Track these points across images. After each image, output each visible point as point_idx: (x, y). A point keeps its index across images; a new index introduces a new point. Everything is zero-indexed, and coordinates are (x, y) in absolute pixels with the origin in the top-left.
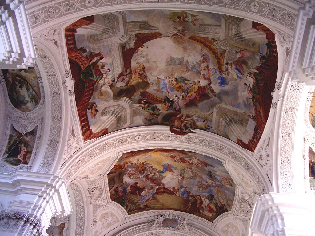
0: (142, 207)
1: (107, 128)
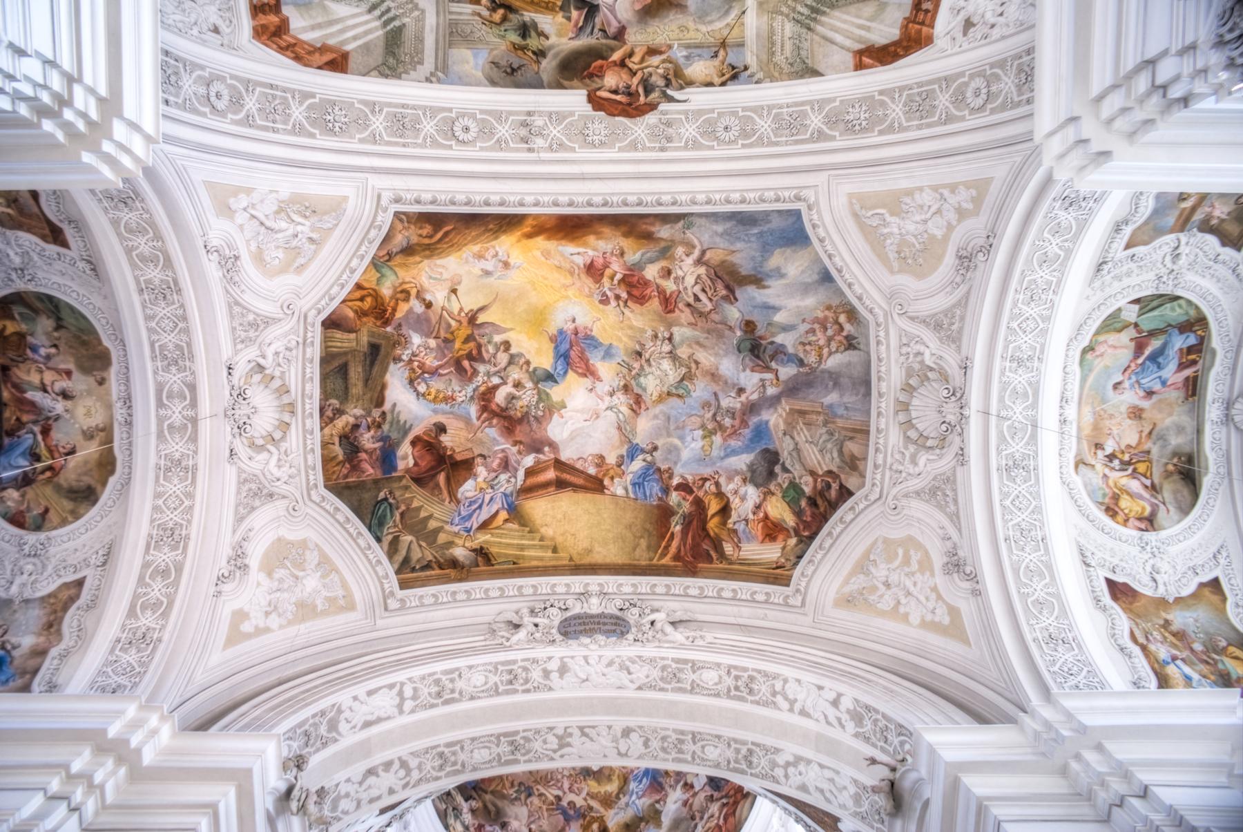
0: (461, 559)
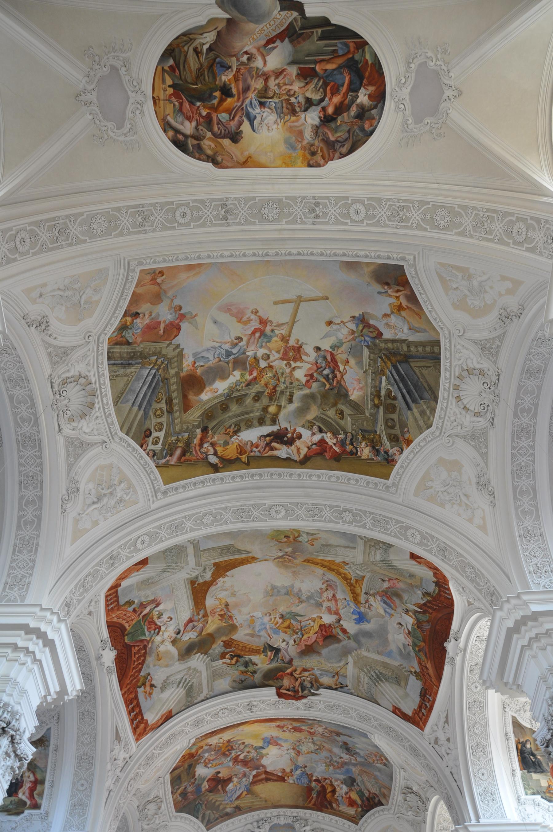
1: (171, 710)
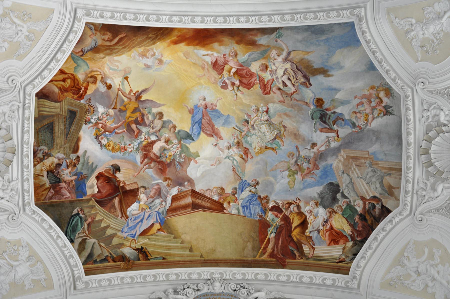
0: (128, 255)
